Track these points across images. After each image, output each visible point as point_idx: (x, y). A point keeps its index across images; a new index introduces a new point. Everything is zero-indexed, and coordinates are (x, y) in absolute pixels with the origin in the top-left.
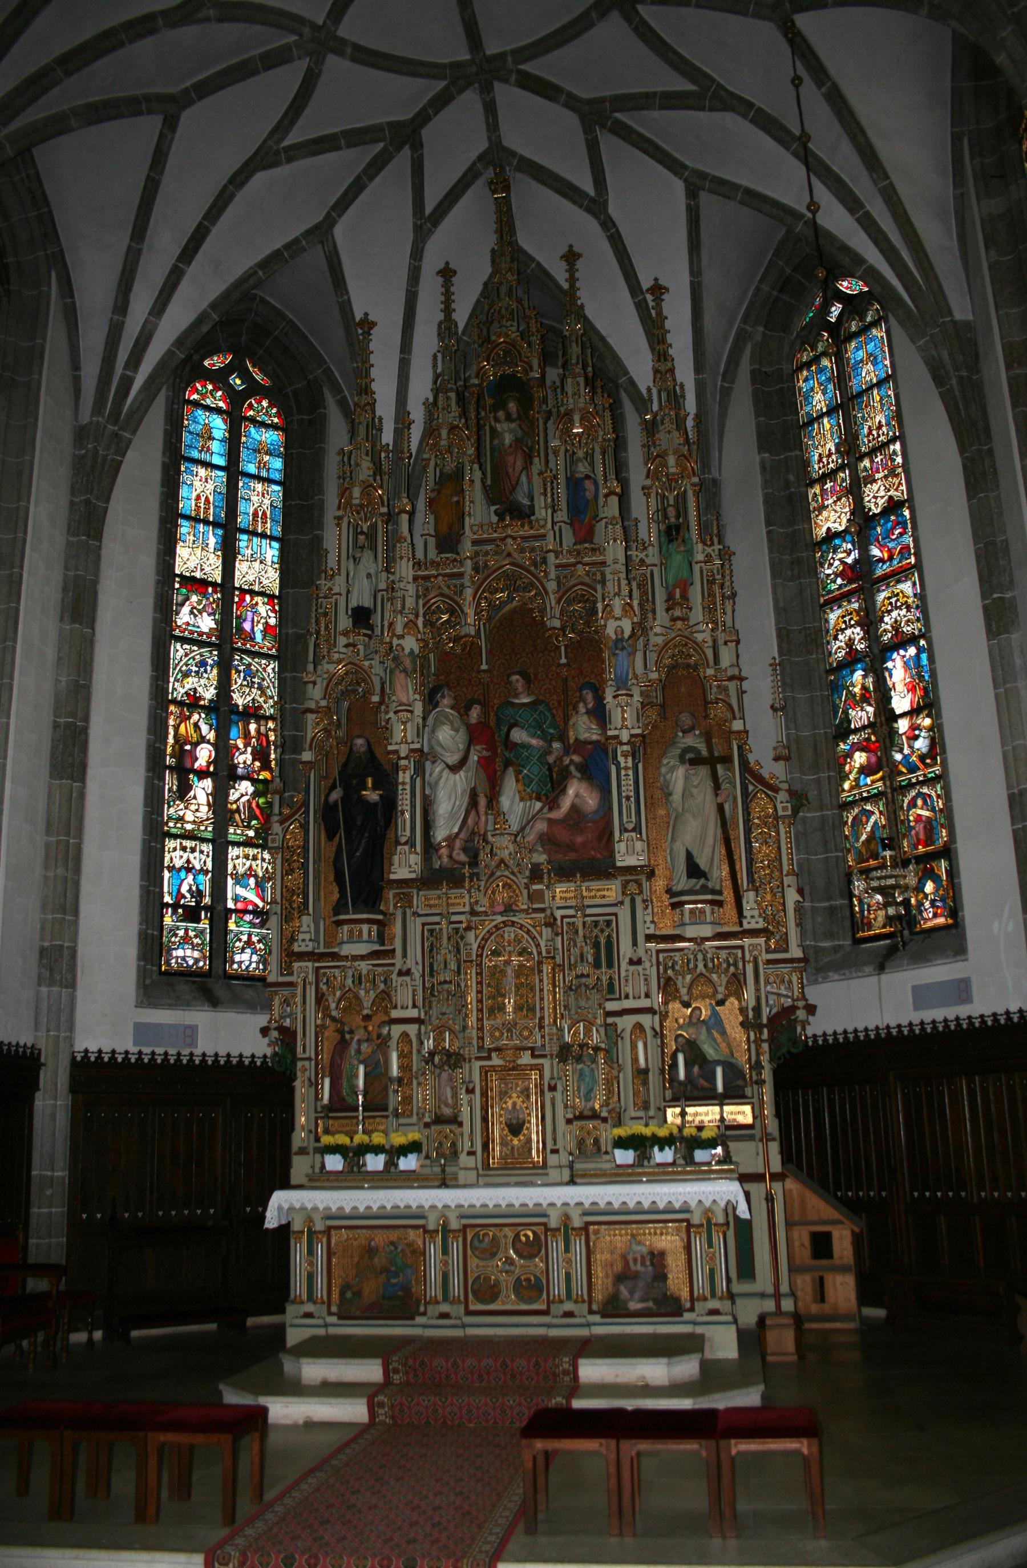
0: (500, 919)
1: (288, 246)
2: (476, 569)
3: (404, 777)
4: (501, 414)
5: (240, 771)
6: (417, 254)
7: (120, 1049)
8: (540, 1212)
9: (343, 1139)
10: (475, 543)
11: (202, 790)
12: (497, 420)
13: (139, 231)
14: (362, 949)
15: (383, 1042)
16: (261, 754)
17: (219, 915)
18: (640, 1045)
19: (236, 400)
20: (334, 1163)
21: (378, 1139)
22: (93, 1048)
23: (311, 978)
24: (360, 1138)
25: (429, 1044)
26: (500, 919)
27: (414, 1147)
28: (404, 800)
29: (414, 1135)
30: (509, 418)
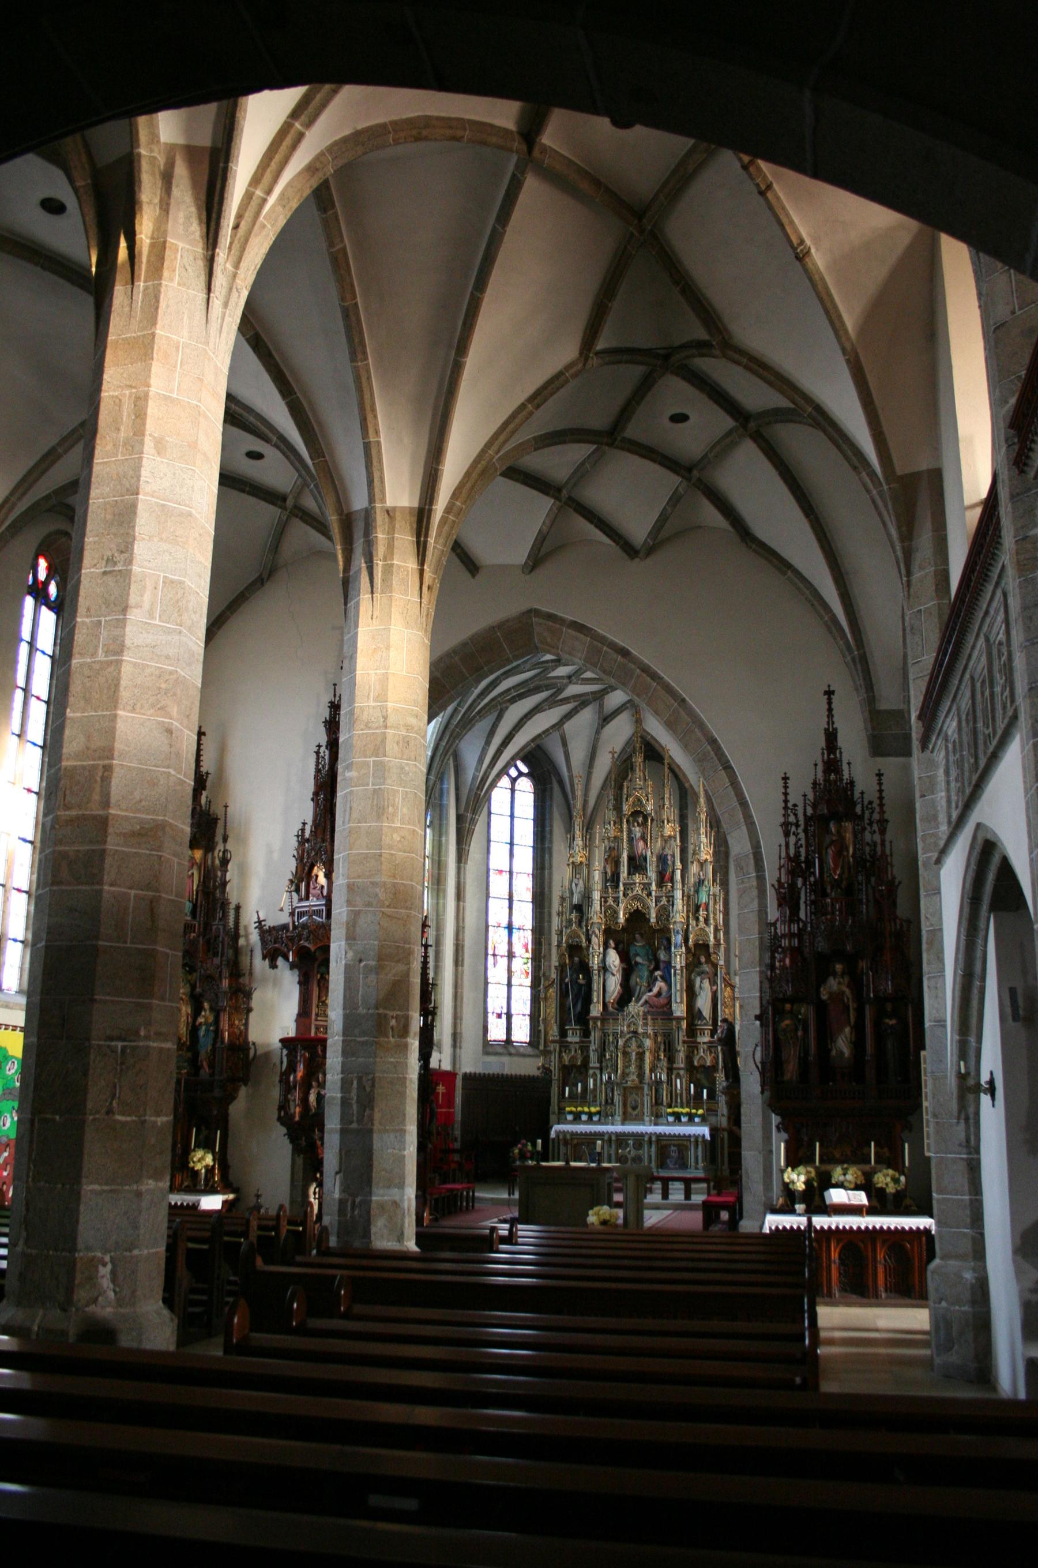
0: (631, 1035)
1: (544, 732)
2: (624, 895)
3: (595, 978)
4: (636, 824)
5: (517, 955)
6: (598, 732)
7: (477, 1072)
8: (642, 1135)
9: (574, 1109)
10: (624, 884)
11: (503, 962)
12: (634, 826)
13: (488, 743)
14: (577, 1039)
15: (587, 1076)
16: (526, 946)
17: (509, 1016)
18: (678, 1081)
19: (514, 780)
20: (570, 1117)
21: (586, 1109)
22: (468, 1071)
23: (558, 1049)
24: (579, 1109)
25: (605, 1078)
26: (631, 1035)
27: (599, 1113)
28: (595, 987)
29: (598, 1109)
30: (638, 825)
